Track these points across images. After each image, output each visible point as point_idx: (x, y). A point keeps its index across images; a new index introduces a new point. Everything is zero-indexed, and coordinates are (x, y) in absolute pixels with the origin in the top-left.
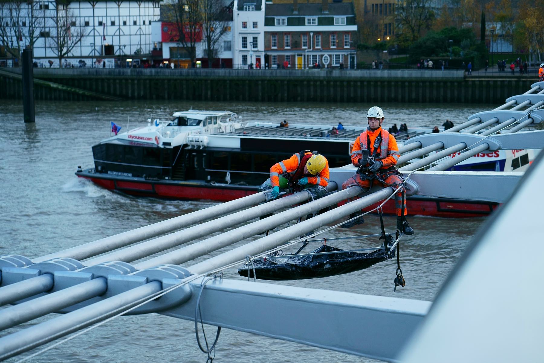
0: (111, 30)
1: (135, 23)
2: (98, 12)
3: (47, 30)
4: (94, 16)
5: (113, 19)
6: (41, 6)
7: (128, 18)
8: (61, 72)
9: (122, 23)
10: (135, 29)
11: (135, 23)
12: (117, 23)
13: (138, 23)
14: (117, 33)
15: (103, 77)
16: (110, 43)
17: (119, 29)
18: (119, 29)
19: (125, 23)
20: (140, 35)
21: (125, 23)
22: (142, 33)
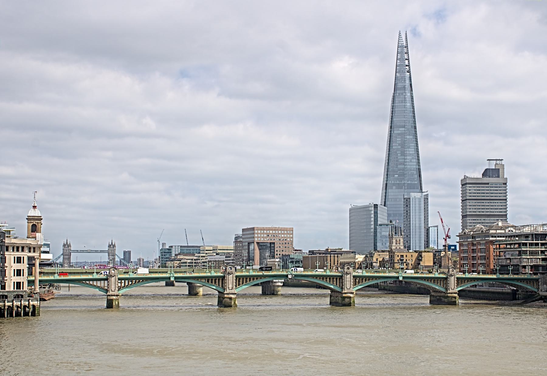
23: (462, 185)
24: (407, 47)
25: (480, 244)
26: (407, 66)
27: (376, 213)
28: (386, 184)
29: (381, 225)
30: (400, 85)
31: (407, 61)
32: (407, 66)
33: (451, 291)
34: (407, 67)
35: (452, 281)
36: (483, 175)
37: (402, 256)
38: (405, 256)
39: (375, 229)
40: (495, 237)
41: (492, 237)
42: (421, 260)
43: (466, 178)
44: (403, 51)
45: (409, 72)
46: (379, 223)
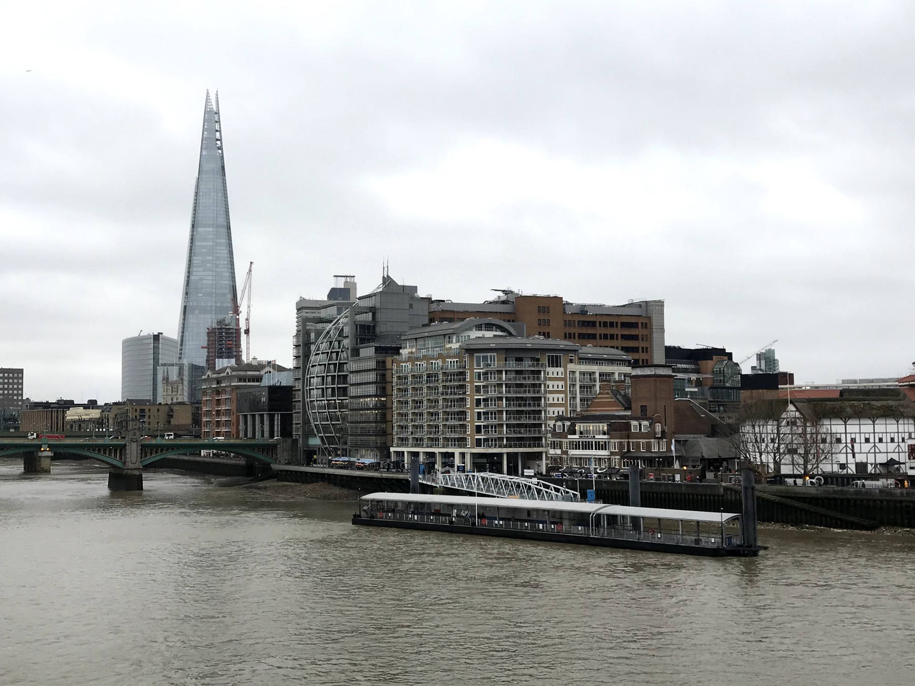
0: (866, 447)
1: (892, 440)
2: (850, 429)
3: (795, 446)
4: (846, 433)
5: (867, 436)
6: (788, 423)
7: (858, 435)
8: (803, 490)
9: (877, 440)
10: (892, 447)
11: (892, 440)
12: (872, 440)
13: (896, 440)
14: (872, 451)
15: (849, 497)
16: (864, 461)
17: (875, 446)
18: (875, 446)
19: (881, 440)
20: (875, 453)
21: (881, 440)
22: (877, 451)
23: (298, 310)
24: (217, 113)
25: (224, 391)
26: (217, 140)
27: (156, 349)
28: (185, 307)
29: (162, 365)
30: (206, 167)
31: (218, 134)
32: (217, 140)
33: (131, 466)
34: (218, 142)
35: (133, 451)
36: (329, 296)
37: (143, 411)
38: (147, 411)
39: (155, 370)
40: (245, 381)
41: (240, 380)
42: (172, 416)
43: (302, 300)
44: (212, 119)
45: (220, 148)
46: (160, 362)
